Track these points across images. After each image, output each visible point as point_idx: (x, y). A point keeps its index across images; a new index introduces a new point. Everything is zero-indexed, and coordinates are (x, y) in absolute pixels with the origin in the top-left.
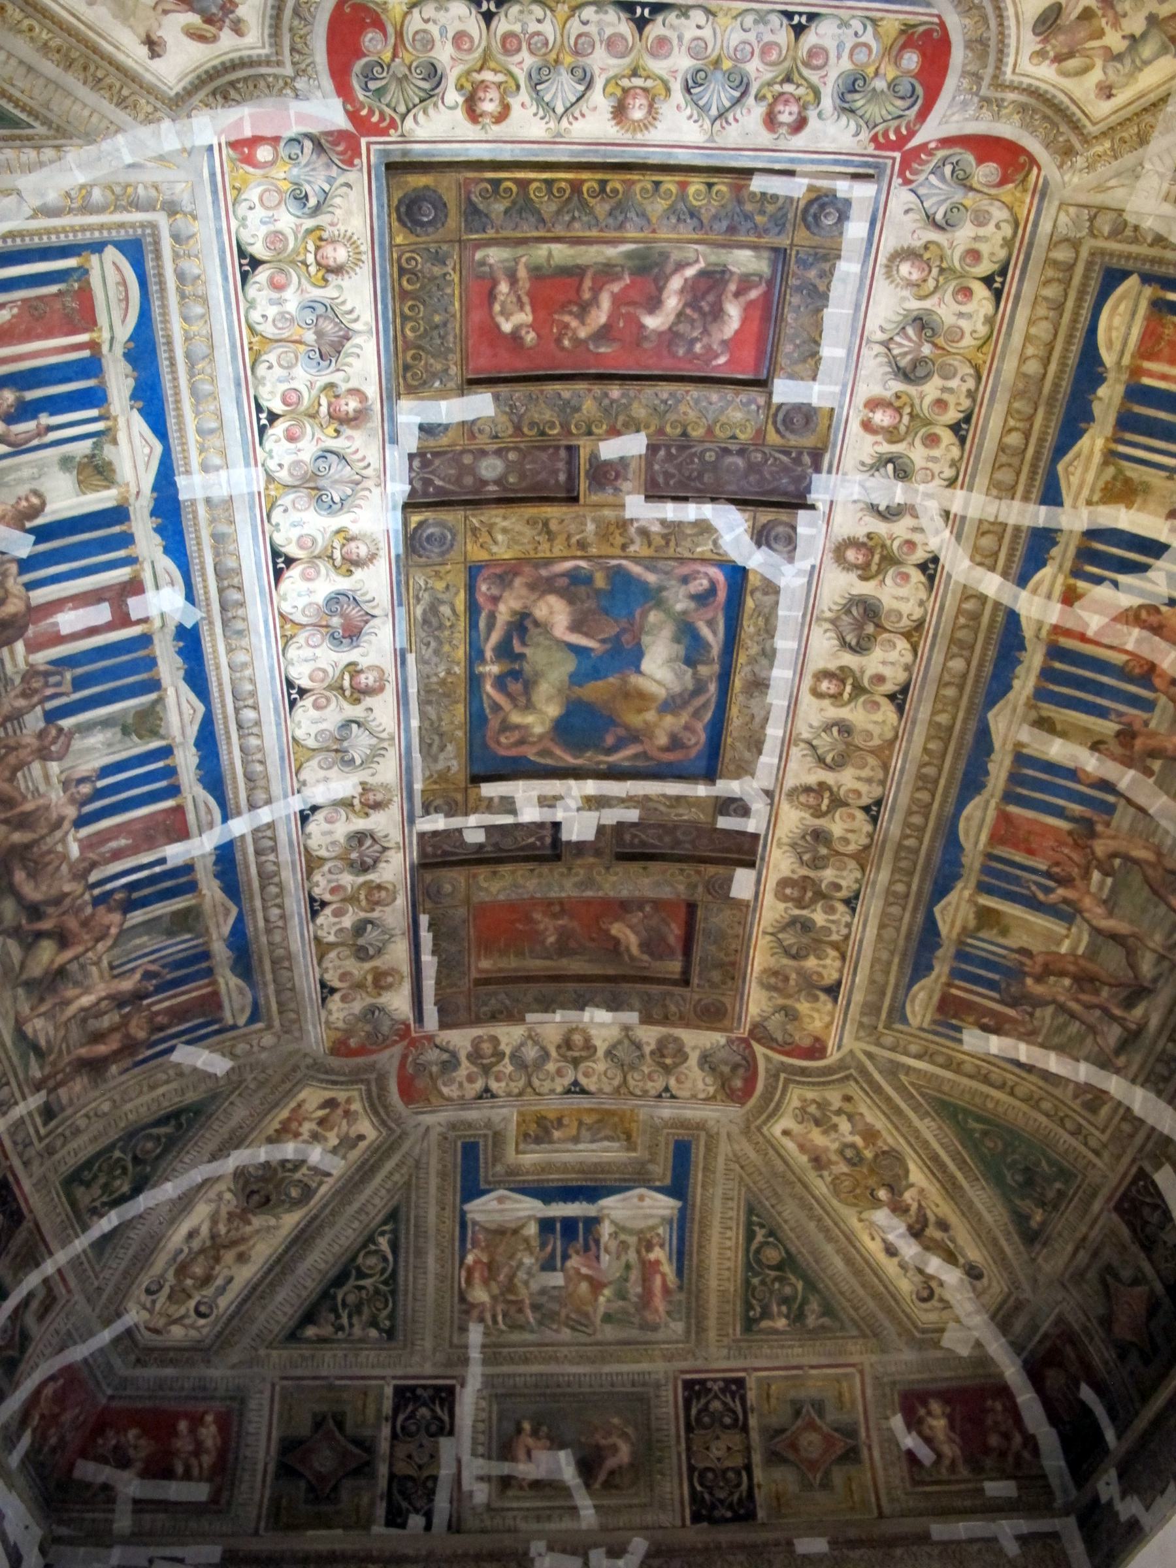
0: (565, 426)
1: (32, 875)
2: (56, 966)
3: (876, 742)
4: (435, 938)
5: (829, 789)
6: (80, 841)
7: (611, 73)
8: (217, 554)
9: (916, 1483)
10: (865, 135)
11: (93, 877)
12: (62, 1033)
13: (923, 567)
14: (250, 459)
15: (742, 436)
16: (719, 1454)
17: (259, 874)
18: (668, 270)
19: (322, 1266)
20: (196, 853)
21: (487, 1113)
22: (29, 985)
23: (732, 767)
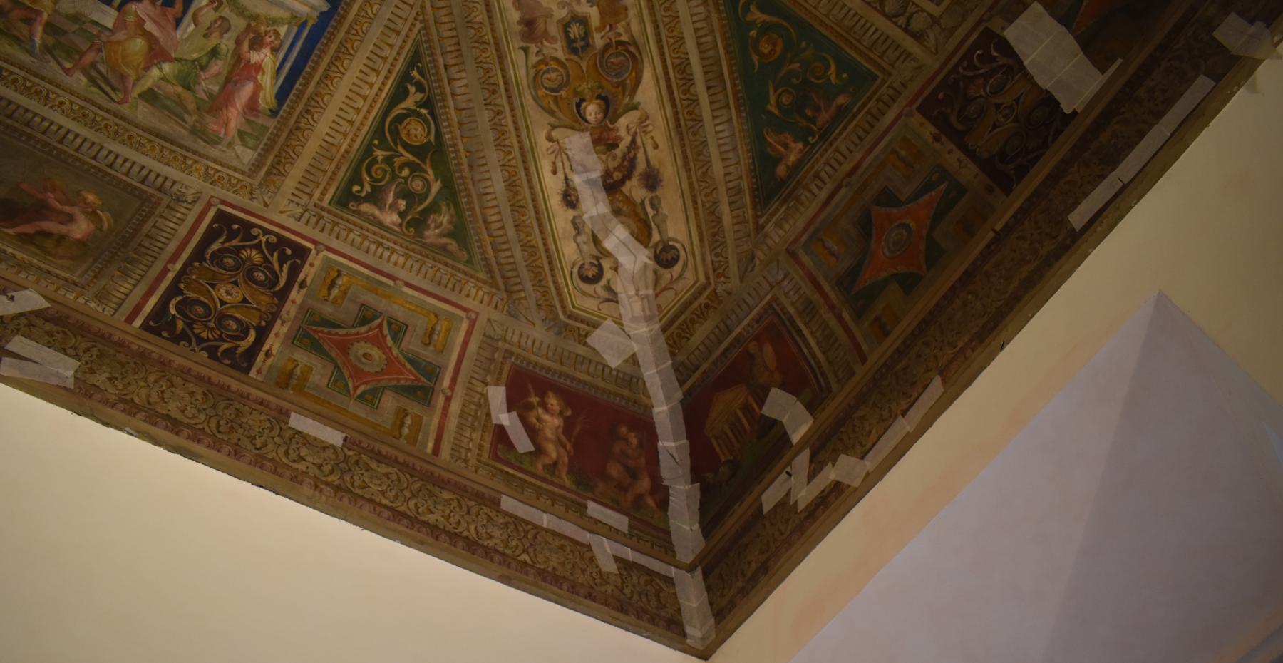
9: (495, 456)
16: (226, 298)
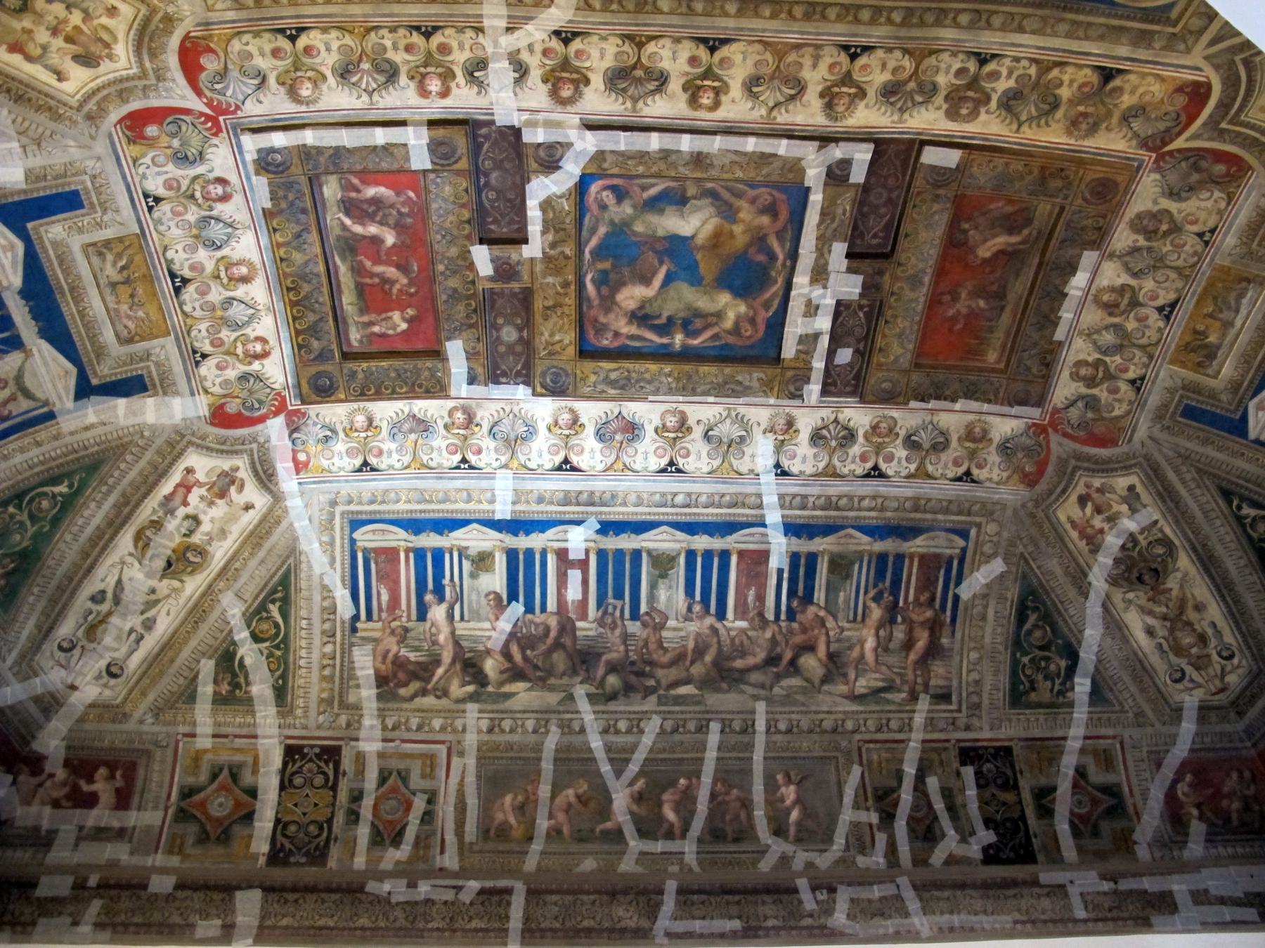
0: (468, 297)
1: (743, 654)
2: (824, 658)
3: (768, 56)
4: (938, 398)
5: (829, 88)
6: (736, 619)
7: (221, 289)
8: (552, 503)
10: (215, 141)
11: (770, 616)
12: (884, 668)
13: (566, 42)
14: (491, 476)
15: (465, 185)
17: (823, 509)
18: (347, 234)
19: (1242, 562)
20: (784, 549)
21: (1157, 388)
22: (826, 680)
23: (791, 176)
